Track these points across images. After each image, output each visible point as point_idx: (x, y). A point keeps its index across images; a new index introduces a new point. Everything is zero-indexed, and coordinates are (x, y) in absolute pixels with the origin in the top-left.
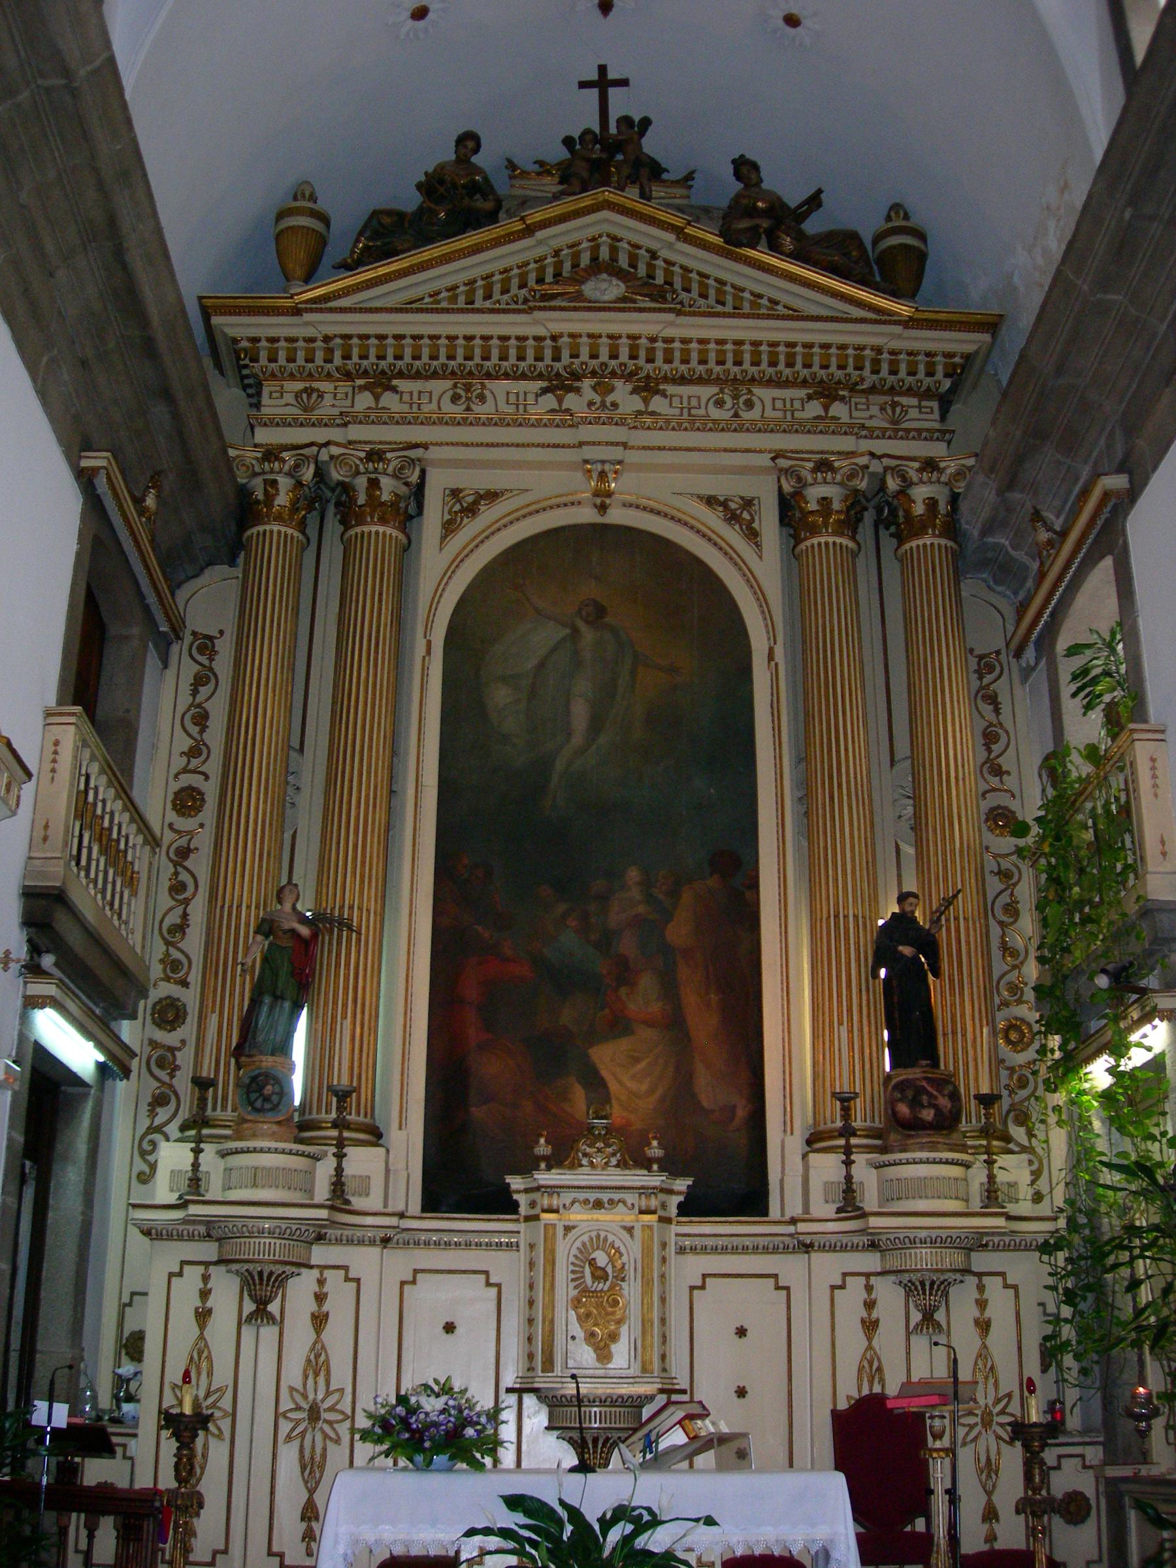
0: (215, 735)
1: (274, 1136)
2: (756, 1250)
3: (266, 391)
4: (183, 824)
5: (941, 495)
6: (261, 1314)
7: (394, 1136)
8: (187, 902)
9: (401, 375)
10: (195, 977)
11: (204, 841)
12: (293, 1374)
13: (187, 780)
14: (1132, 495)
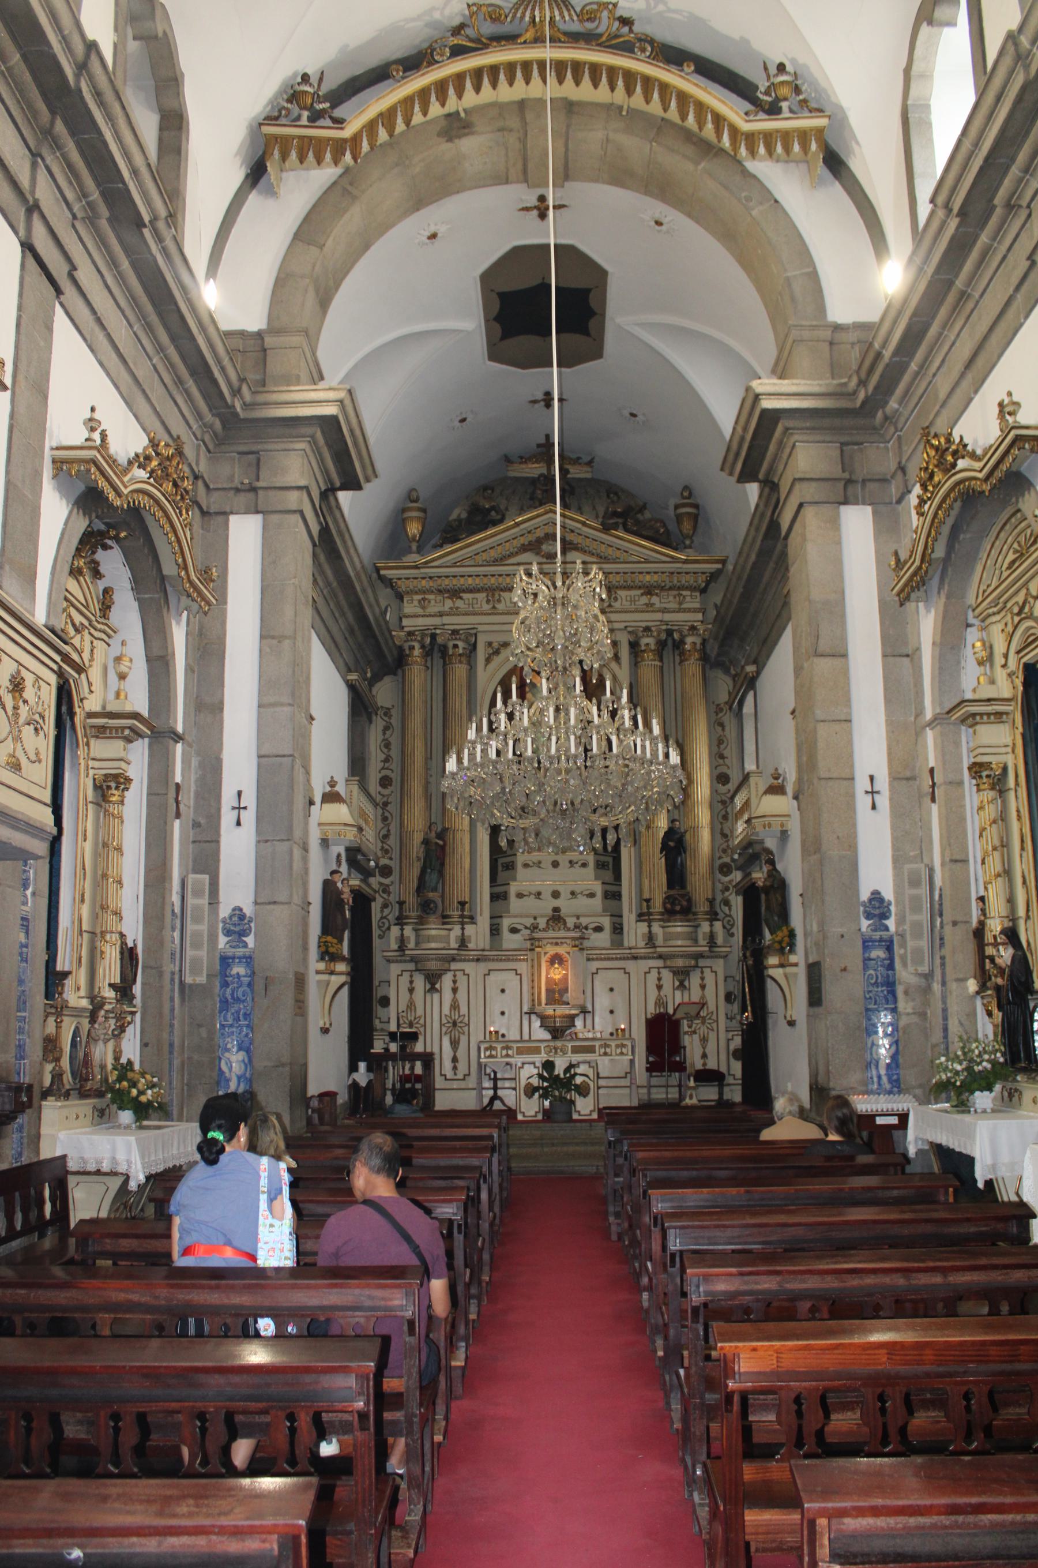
0: (395, 752)
1: (434, 923)
2: (617, 959)
3: (405, 600)
4: (386, 792)
5: (698, 641)
6: (433, 989)
7: (479, 919)
8: (389, 825)
9: (464, 591)
10: (395, 854)
11: (394, 799)
12: (446, 1010)
13: (385, 773)
14: (758, 673)
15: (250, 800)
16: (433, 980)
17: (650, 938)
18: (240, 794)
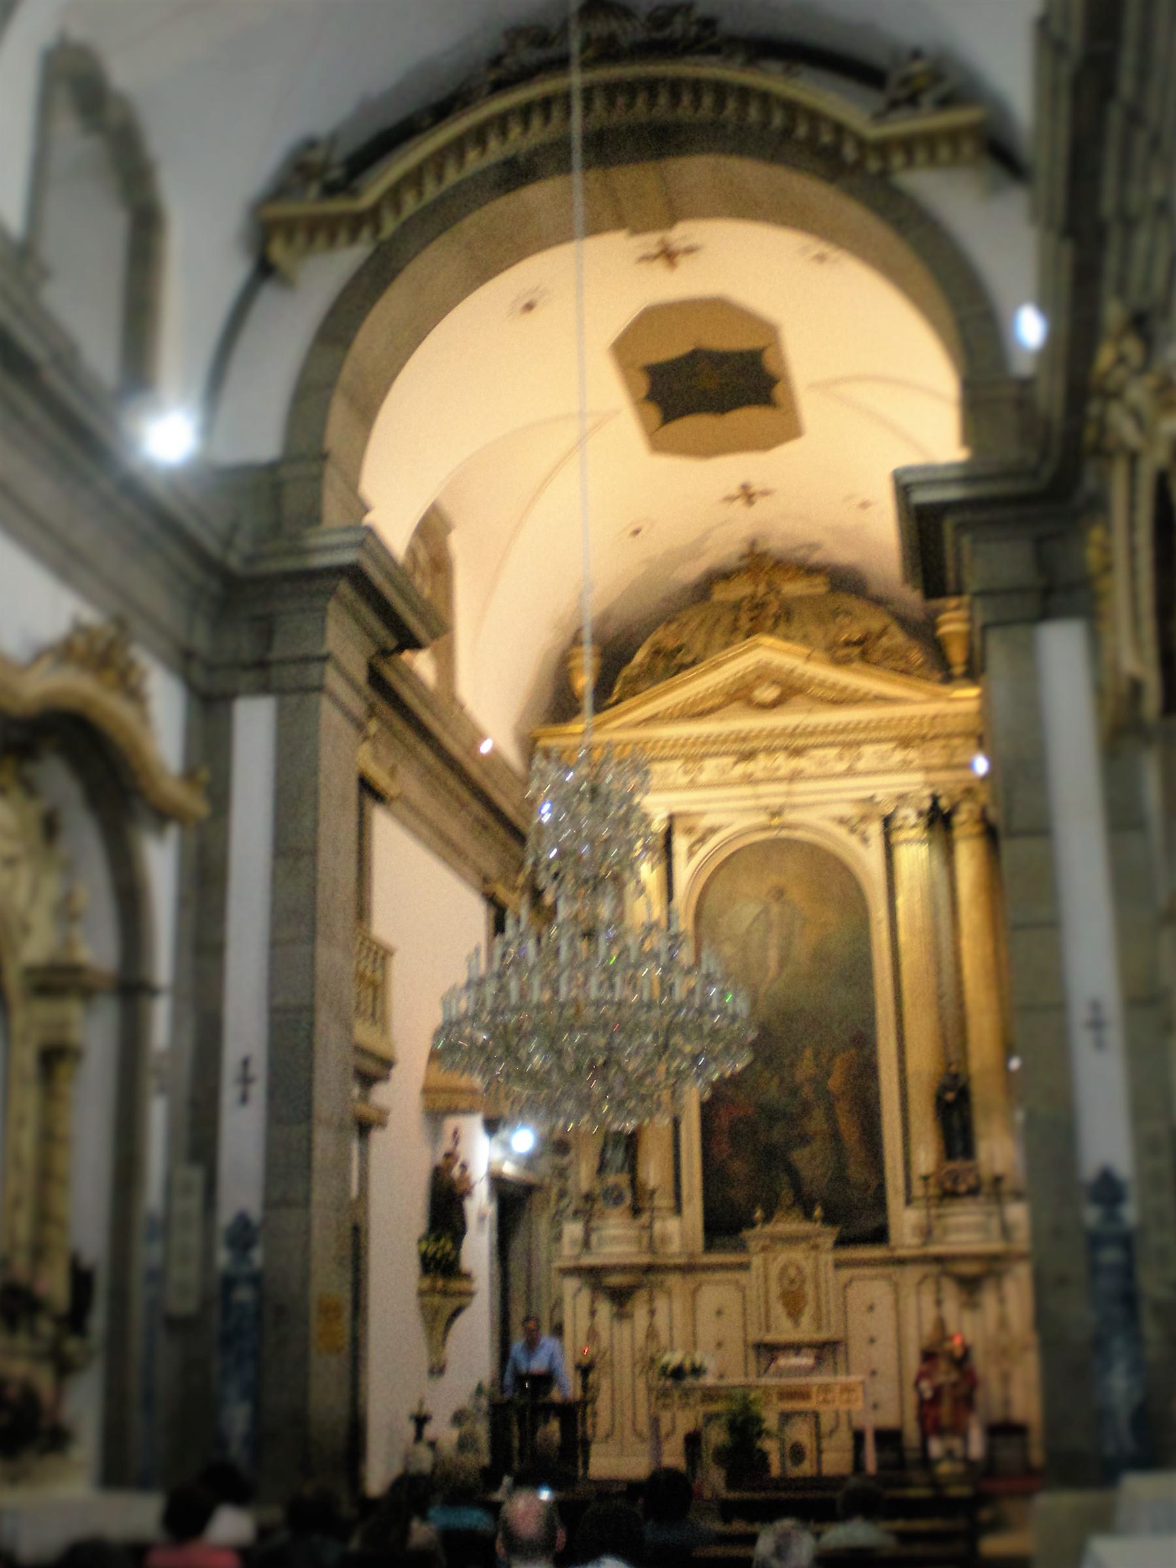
15: (259, 1069)
16: (621, 1297)
17: (927, 1233)
18: (246, 1063)
